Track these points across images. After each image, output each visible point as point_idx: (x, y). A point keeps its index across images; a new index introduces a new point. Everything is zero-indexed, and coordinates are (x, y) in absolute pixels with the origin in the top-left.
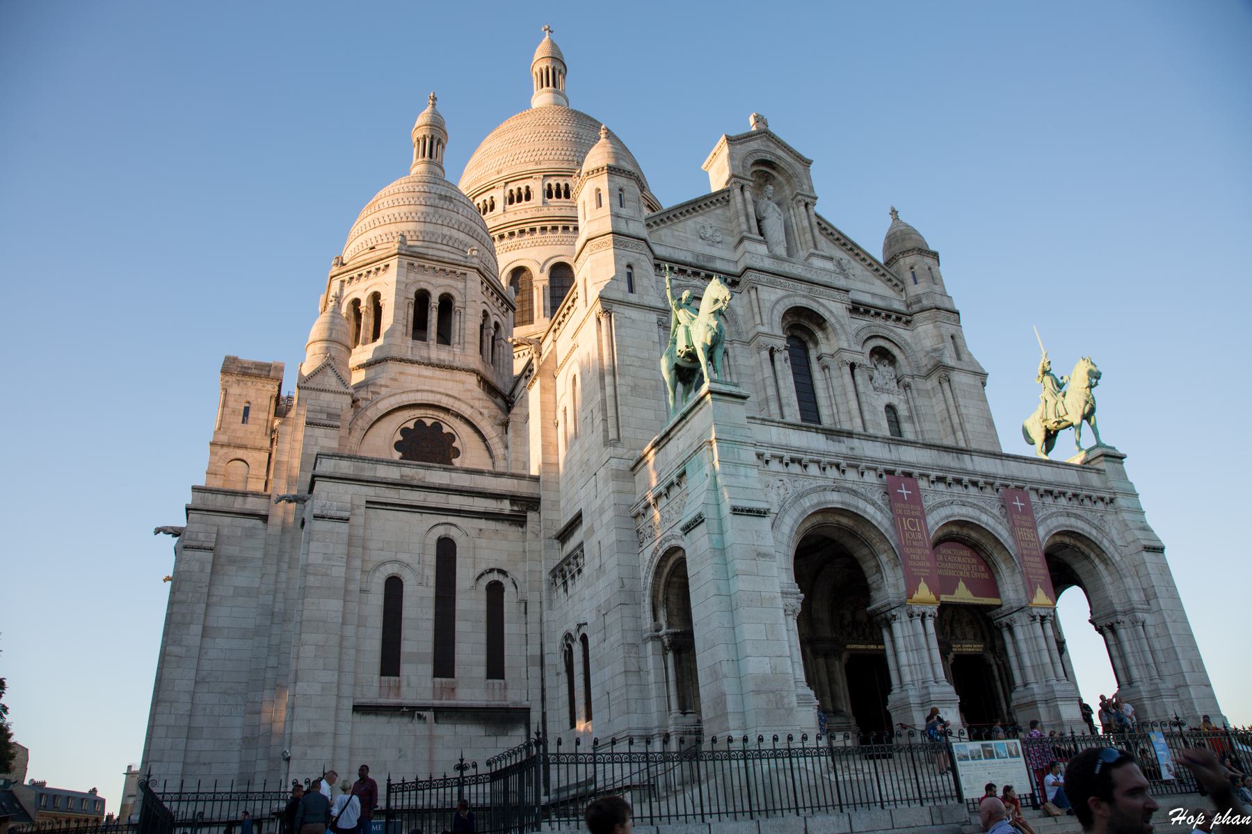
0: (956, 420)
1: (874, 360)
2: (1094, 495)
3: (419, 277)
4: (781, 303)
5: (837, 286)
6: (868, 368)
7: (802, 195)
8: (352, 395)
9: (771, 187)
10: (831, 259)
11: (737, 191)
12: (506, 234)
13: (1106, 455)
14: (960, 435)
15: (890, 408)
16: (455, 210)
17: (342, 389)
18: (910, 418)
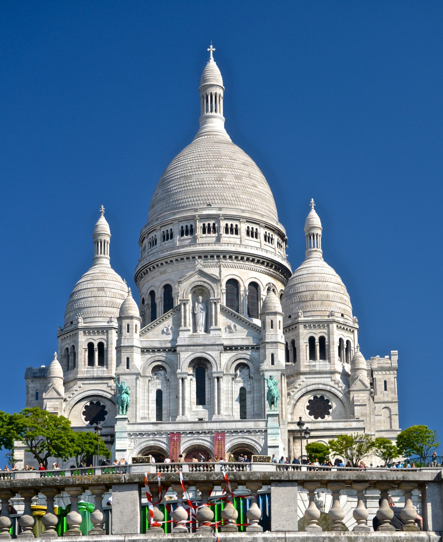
0: (263, 393)
1: (239, 368)
2: (257, 430)
3: (89, 337)
4: (189, 357)
5: (217, 343)
6: (231, 375)
7: (212, 299)
8: (62, 398)
9: (200, 298)
10: (220, 329)
11: (183, 306)
12: (159, 264)
13: (269, 415)
14: (263, 398)
15: (242, 390)
16: (105, 296)
17: (58, 397)
18: (250, 392)
